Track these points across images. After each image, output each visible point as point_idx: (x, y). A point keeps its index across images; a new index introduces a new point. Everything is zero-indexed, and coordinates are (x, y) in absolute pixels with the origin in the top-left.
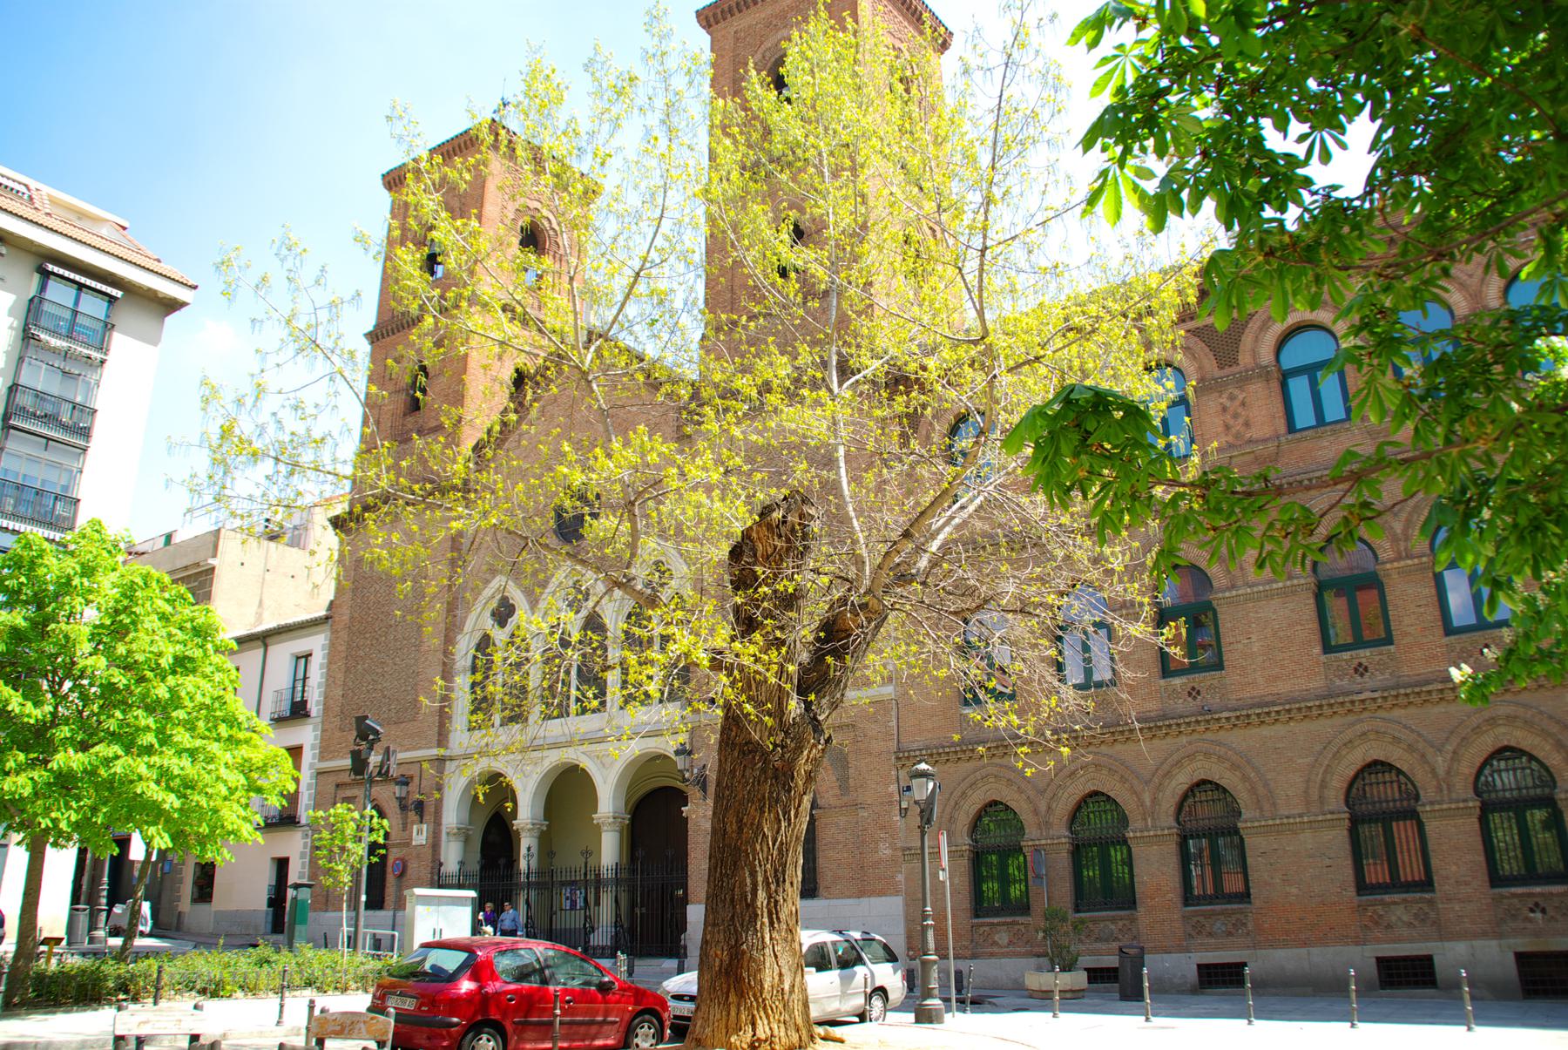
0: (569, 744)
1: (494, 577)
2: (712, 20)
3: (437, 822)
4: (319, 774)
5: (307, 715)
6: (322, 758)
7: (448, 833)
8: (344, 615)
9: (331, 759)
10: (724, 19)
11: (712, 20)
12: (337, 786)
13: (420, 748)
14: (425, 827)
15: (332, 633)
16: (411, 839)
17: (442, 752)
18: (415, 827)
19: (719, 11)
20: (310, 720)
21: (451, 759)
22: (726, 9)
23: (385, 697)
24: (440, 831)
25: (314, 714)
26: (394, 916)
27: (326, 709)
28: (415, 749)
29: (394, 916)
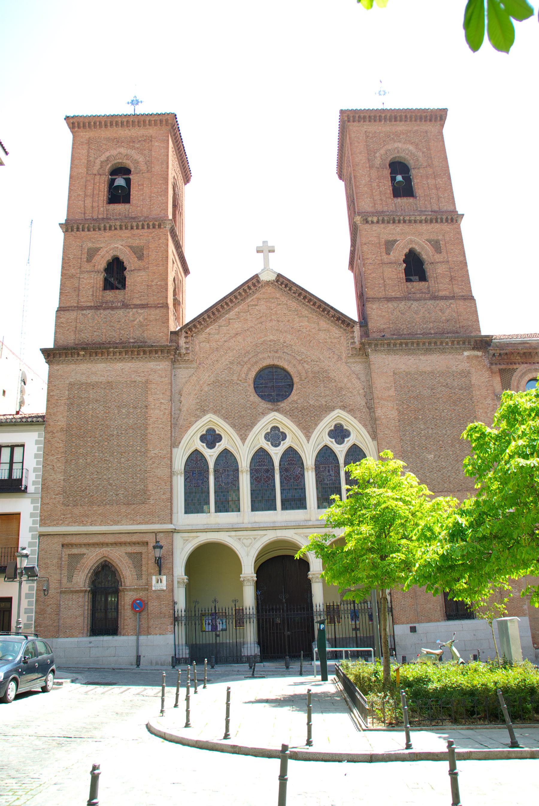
0: (286, 528)
1: (205, 415)
2: (351, 119)
3: (171, 574)
4: (40, 536)
5: (25, 490)
6: (43, 522)
7: (178, 582)
8: (61, 421)
9: (54, 525)
10: (359, 121)
11: (351, 119)
12: (63, 545)
13: (152, 523)
14: (164, 578)
15: (47, 432)
16: (151, 586)
17: (170, 527)
18: (154, 578)
19: (357, 116)
20: (27, 495)
21: (178, 532)
22: (362, 116)
23: (111, 484)
24: (173, 581)
25: (31, 489)
26: (138, 639)
27: (45, 487)
28: (147, 523)
29: (138, 639)
